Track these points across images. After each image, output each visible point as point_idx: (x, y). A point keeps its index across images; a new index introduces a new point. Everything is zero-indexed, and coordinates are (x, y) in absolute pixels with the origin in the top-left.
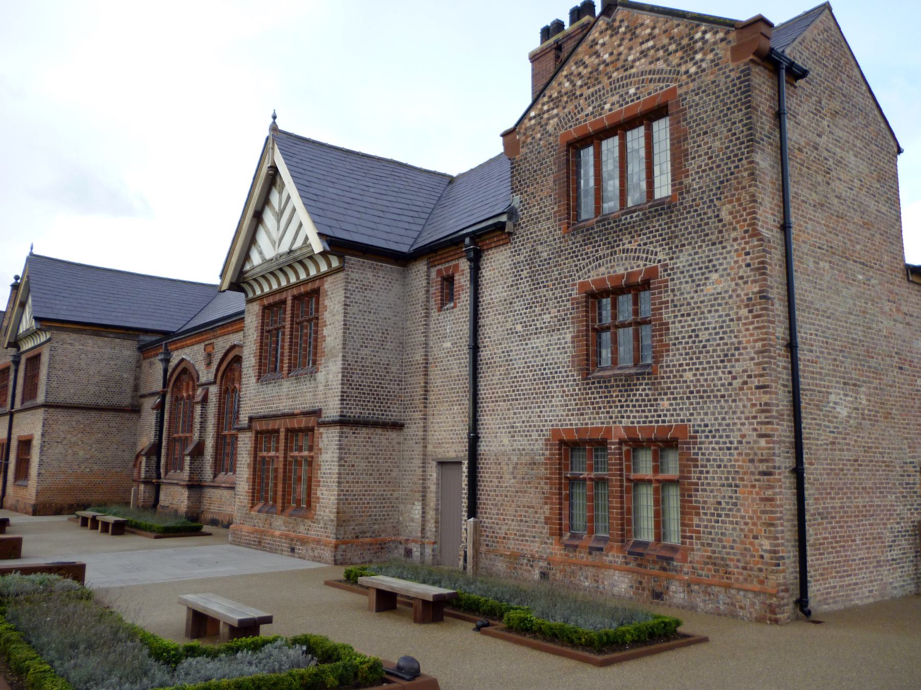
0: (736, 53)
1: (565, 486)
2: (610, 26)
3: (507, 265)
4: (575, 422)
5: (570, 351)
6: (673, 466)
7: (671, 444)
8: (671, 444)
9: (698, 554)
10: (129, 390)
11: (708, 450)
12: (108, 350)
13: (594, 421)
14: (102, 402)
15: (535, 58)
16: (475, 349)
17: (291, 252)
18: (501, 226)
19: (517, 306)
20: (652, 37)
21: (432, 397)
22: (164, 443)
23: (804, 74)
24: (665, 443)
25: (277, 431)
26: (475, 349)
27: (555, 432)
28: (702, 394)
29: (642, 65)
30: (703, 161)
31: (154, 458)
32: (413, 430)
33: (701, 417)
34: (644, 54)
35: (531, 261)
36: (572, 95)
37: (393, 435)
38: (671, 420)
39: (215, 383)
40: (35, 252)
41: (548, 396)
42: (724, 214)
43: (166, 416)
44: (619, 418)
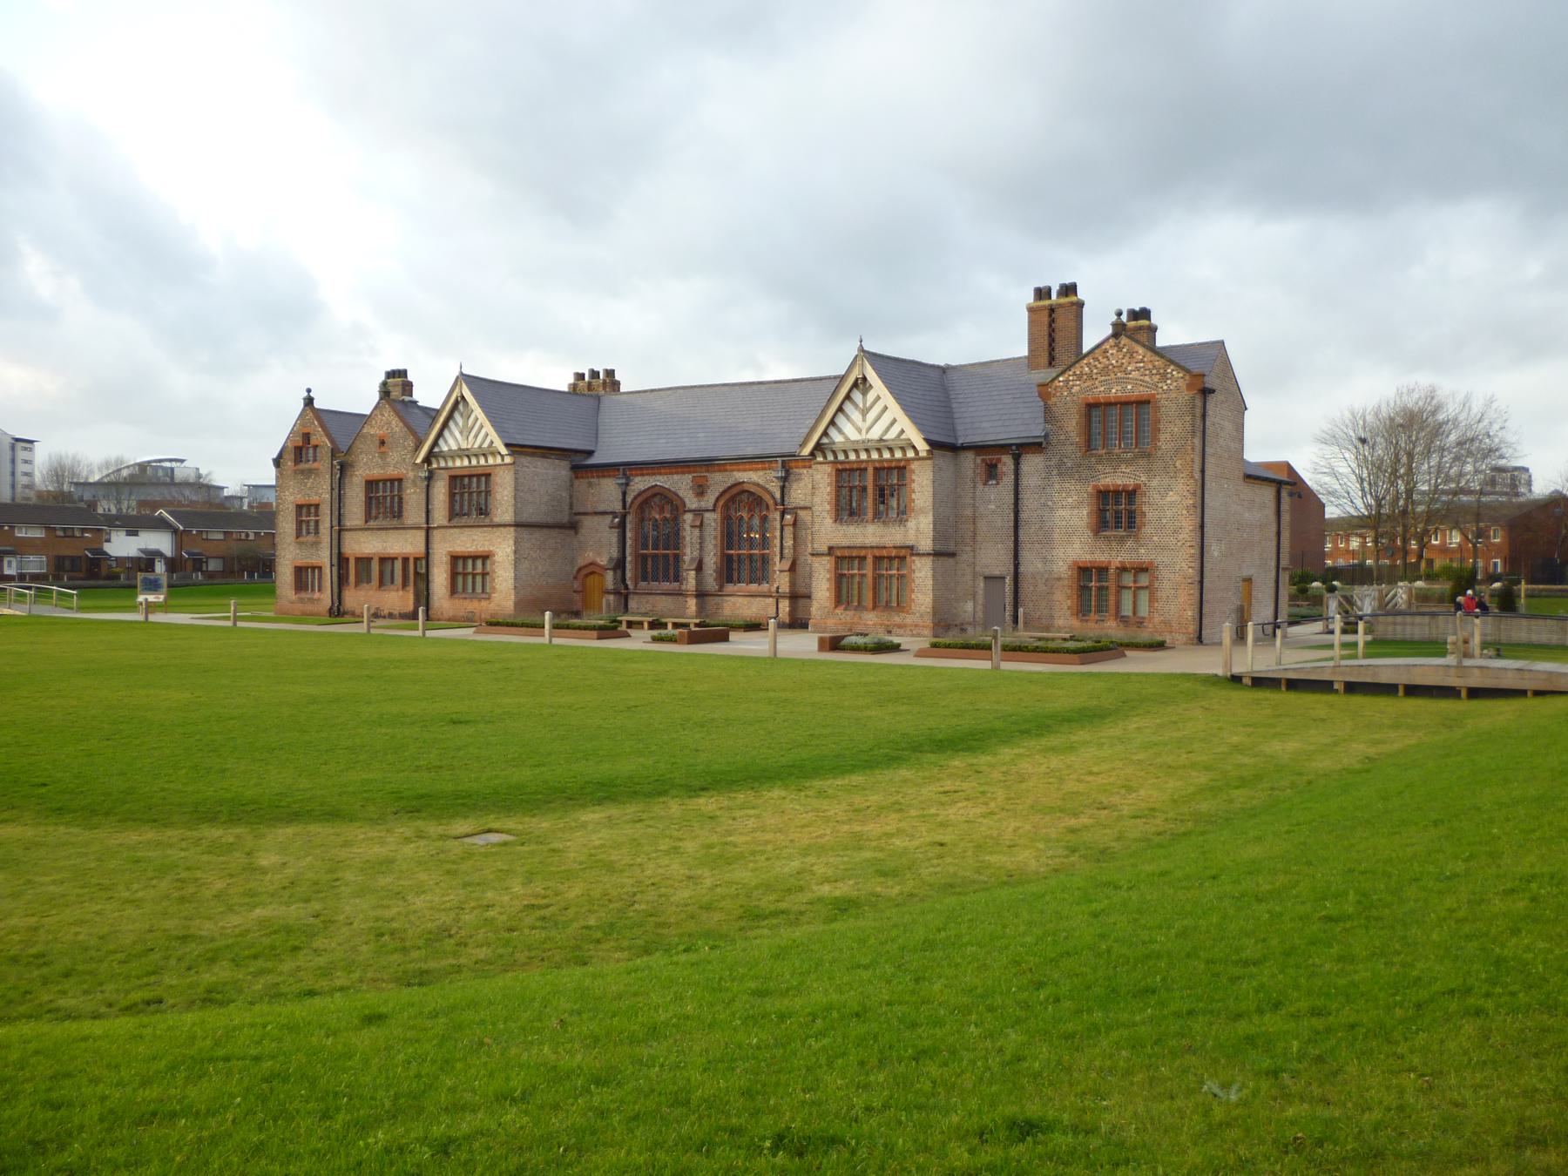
0: (1189, 387)
1: (1083, 590)
2: (1116, 345)
3: (1041, 466)
4: (1088, 557)
5: (1086, 520)
6: (1144, 580)
7: (1145, 570)
8: (1145, 570)
9: (1157, 619)
10: (567, 511)
11: (1164, 573)
12: (551, 471)
13: (1101, 557)
14: (550, 520)
15: (1031, 310)
17: (881, 440)
18: (1040, 444)
21: (979, 538)
22: (629, 559)
23: (1213, 391)
24: (1142, 569)
25: (864, 558)
27: (1075, 563)
28: (1163, 548)
30: (1168, 436)
31: (619, 572)
32: (965, 557)
33: (1160, 558)
34: (1138, 369)
35: (1061, 464)
36: (1090, 376)
37: (951, 560)
38: (1146, 559)
43: (629, 535)
44: (1114, 555)
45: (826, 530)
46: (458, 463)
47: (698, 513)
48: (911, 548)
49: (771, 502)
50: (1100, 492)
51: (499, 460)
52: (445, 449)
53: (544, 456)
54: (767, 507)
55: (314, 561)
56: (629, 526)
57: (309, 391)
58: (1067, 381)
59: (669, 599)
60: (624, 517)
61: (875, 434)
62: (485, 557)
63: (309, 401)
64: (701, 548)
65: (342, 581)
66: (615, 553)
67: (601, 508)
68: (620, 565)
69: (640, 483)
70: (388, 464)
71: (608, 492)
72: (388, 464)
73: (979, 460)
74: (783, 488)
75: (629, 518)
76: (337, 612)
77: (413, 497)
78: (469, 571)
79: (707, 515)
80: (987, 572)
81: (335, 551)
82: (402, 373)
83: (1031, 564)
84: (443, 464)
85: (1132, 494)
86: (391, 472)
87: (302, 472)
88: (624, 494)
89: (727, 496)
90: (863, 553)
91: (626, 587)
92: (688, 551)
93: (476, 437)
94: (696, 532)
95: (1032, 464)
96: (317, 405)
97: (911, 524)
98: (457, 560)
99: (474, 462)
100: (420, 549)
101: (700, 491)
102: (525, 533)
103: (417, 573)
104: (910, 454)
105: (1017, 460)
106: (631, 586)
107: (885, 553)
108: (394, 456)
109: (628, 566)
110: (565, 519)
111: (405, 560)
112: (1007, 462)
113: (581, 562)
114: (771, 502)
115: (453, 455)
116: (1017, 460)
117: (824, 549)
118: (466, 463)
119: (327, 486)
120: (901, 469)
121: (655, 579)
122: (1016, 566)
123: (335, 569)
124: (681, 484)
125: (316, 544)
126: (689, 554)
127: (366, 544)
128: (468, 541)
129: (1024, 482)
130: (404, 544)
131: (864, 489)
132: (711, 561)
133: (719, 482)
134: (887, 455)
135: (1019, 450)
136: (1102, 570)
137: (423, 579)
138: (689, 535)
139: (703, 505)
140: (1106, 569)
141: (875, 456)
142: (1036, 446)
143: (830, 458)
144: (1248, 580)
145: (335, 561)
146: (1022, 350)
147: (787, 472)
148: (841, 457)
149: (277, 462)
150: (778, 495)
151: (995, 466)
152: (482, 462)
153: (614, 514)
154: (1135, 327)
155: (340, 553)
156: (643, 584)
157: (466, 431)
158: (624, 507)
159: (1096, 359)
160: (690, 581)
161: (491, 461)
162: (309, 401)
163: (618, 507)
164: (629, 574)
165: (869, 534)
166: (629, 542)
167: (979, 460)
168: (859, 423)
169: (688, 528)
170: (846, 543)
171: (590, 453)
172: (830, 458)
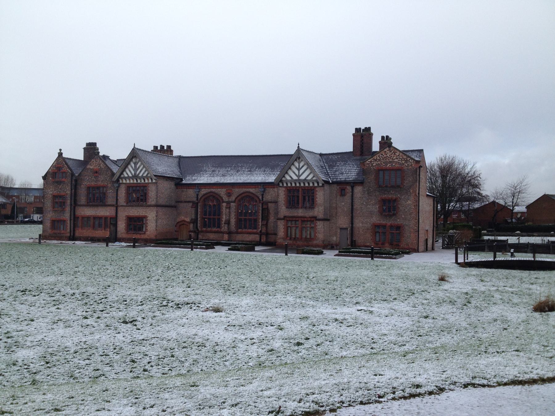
13: (383, 222)
14: (167, 204)
15: (354, 135)
16: (352, 206)
17: (305, 179)
19: (364, 199)
20: (398, 156)
22: (199, 219)
24: (398, 228)
26: (352, 206)
29: (396, 160)
31: (195, 224)
36: (380, 160)
37: (328, 222)
39: (234, 202)
40: (136, 147)
41: (372, 217)
42: (411, 191)
43: (199, 210)
44: (389, 222)
45: (284, 211)
46: (132, 181)
47: (228, 203)
48: (315, 217)
49: (258, 200)
50: (383, 200)
51: (150, 181)
52: (126, 176)
53: (167, 180)
54: (256, 201)
55: (62, 218)
56: (199, 207)
57: (60, 150)
58: (371, 162)
59: (216, 234)
60: (197, 203)
61: (303, 177)
62: (145, 217)
63: (60, 154)
64: (229, 216)
65: (75, 226)
66: (193, 217)
67: (188, 200)
68: (195, 221)
69: (204, 191)
70: (99, 181)
71: (191, 194)
72: (99, 181)
73: (338, 187)
74: (263, 195)
75: (199, 204)
77: (110, 193)
79: (232, 204)
80: (341, 226)
81: (72, 214)
82: (94, 144)
83: (358, 224)
84: (124, 181)
85: (395, 200)
86: (100, 183)
87: (57, 182)
88: (198, 195)
89: (240, 197)
90: (297, 219)
91: (198, 230)
92: (224, 217)
93: (141, 171)
94: (228, 210)
95: (358, 190)
96: (64, 156)
97: (316, 209)
99: (139, 181)
100: (113, 214)
101: (229, 195)
102: (160, 209)
104: (316, 185)
105: (352, 188)
106: (200, 230)
107: (306, 219)
108: (101, 178)
109: (199, 222)
110: (173, 203)
111: (106, 218)
112: (349, 188)
113: (178, 220)
114: (258, 200)
115: (129, 178)
116: (352, 188)
117: (282, 217)
118: (135, 181)
119: (69, 188)
121: (210, 227)
122: (352, 224)
123: (72, 221)
124: (222, 192)
125: (63, 210)
126: (224, 218)
127: (89, 212)
128: (135, 212)
129: (355, 196)
130: (105, 212)
131: (298, 197)
132: (233, 221)
133: (237, 191)
134: (307, 185)
135: (353, 184)
136: (384, 226)
137: (115, 225)
138: (224, 210)
139: (230, 200)
140: (385, 226)
141: (302, 185)
142: (361, 183)
143: (285, 185)
144: (427, 231)
145: (72, 218)
146: (350, 149)
147: (265, 189)
148: (289, 185)
149: (44, 178)
150: (260, 198)
151: (344, 190)
152: (143, 181)
153: (193, 202)
154: (386, 142)
155: (74, 215)
156: (204, 229)
157: (136, 169)
158: (197, 200)
159: (382, 154)
160: (225, 228)
161: (146, 181)
162: (60, 154)
163: (195, 199)
164: (199, 225)
165: (300, 212)
166: (199, 213)
167: (338, 187)
168: (297, 174)
169: (224, 208)
170: (291, 215)
171: (182, 180)
172: (285, 185)
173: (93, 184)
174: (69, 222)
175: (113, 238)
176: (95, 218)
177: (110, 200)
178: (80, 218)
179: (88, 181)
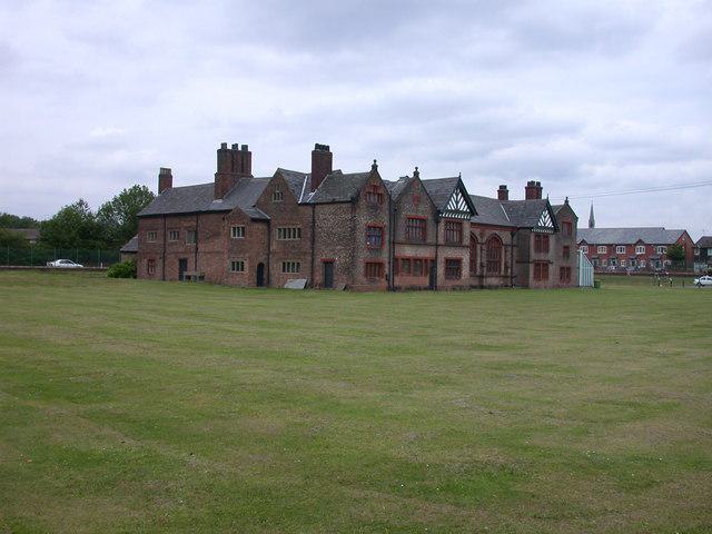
24: (569, 269)
76: (393, 289)
78: (453, 266)
98: (458, 262)
101: (482, 235)
103: (429, 266)
111: (426, 260)
115: (451, 211)
120: (546, 236)
127: (409, 252)
128: (452, 253)
130: (425, 253)
133: (489, 232)
157: (457, 203)
173: (413, 214)
174: (387, 265)
175: (433, 286)
176: (416, 260)
177: (430, 239)
178: (400, 261)
179: (408, 210)
